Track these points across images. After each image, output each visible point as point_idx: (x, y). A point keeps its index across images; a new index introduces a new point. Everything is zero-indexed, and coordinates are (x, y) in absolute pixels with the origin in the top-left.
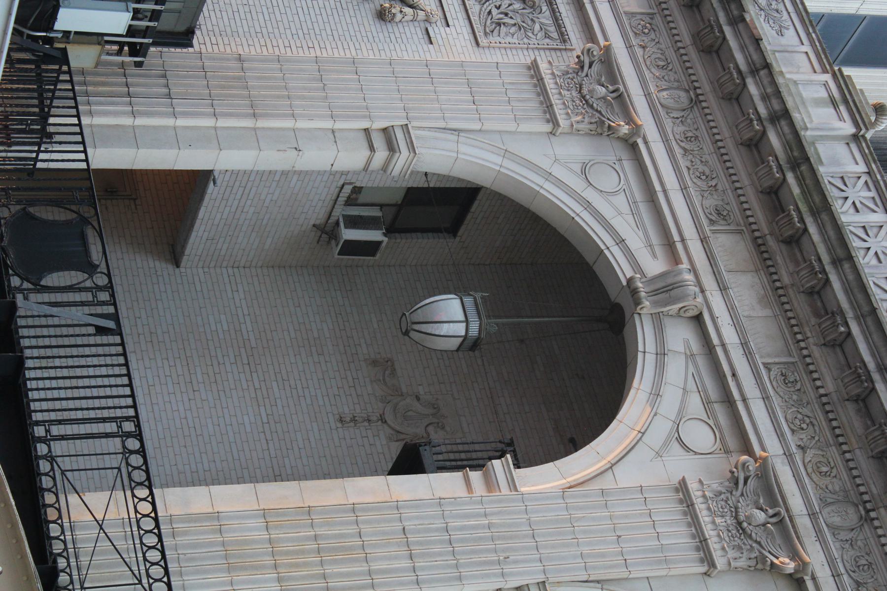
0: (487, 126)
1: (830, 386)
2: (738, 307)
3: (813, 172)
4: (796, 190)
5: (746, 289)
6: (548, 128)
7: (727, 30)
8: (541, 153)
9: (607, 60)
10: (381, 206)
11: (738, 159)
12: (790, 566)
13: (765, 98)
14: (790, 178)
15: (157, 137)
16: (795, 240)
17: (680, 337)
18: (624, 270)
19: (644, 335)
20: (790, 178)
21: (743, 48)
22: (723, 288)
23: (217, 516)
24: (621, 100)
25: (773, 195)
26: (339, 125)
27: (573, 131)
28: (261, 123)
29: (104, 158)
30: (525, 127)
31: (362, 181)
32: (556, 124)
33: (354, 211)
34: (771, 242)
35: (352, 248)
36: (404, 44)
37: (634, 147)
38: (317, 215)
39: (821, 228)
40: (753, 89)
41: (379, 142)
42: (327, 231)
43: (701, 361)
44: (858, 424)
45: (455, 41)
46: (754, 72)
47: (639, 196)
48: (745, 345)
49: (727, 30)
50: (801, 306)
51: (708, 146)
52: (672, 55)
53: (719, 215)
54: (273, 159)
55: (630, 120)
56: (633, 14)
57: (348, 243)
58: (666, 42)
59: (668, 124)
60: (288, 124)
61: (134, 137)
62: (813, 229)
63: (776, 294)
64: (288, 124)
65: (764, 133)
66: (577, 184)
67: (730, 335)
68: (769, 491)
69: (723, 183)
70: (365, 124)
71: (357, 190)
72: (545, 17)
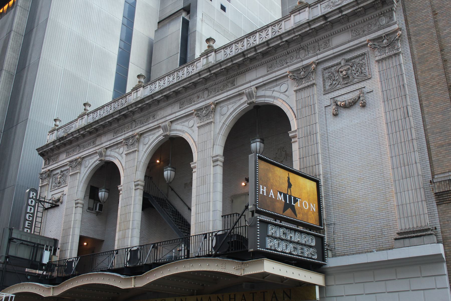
0: (77, 185)
1: (116, 125)
2: (106, 141)
3: (86, 126)
4: (89, 129)
5: (104, 139)
6: (79, 174)
7: (67, 139)
8: (82, 175)
9: (71, 162)
10: (94, 203)
11: (86, 139)
12: (137, 136)
13: (76, 134)
14: (87, 130)
15: (72, 246)
16: (97, 130)
17: (109, 152)
18: (98, 162)
19: (108, 159)
20: (87, 130)
21: (70, 137)
22: (102, 144)
23: (118, 239)
24: (76, 160)
25: (90, 133)
26: (74, 212)
27: (80, 169)
28: (72, 227)
29: (75, 254)
30: (78, 178)
31: (86, 207)
32: (78, 172)
33: (94, 209)
34: (97, 134)
35: (101, 208)
36: (65, 199)
37: (83, 158)
38: (93, 216)
39: (94, 125)
40: (75, 136)
41: (77, 205)
42: (97, 214)
43: (112, 148)
44: (122, 121)
45: (66, 189)
46: (73, 135)
47: (89, 158)
48: (110, 140)
49: (67, 139)
50: (106, 129)
51: (85, 144)
52: (72, 149)
53: (94, 142)
54: (78, 225)
55: (78, 159)
56: (66, 156)
57: (99, 210)
58: (70, 150)
59: (81, 151)
60: (72, 222)
61: (71, 250)
62: (94, 127)
63: (105, 133)
64: (72, 222)
65: (81, 134)
66: (87, 168)
67: (108, 143)
68: (127, 139)
69: (90, 141)
70: (74, 208)
71: (89, 208)
72: (65, 172)
